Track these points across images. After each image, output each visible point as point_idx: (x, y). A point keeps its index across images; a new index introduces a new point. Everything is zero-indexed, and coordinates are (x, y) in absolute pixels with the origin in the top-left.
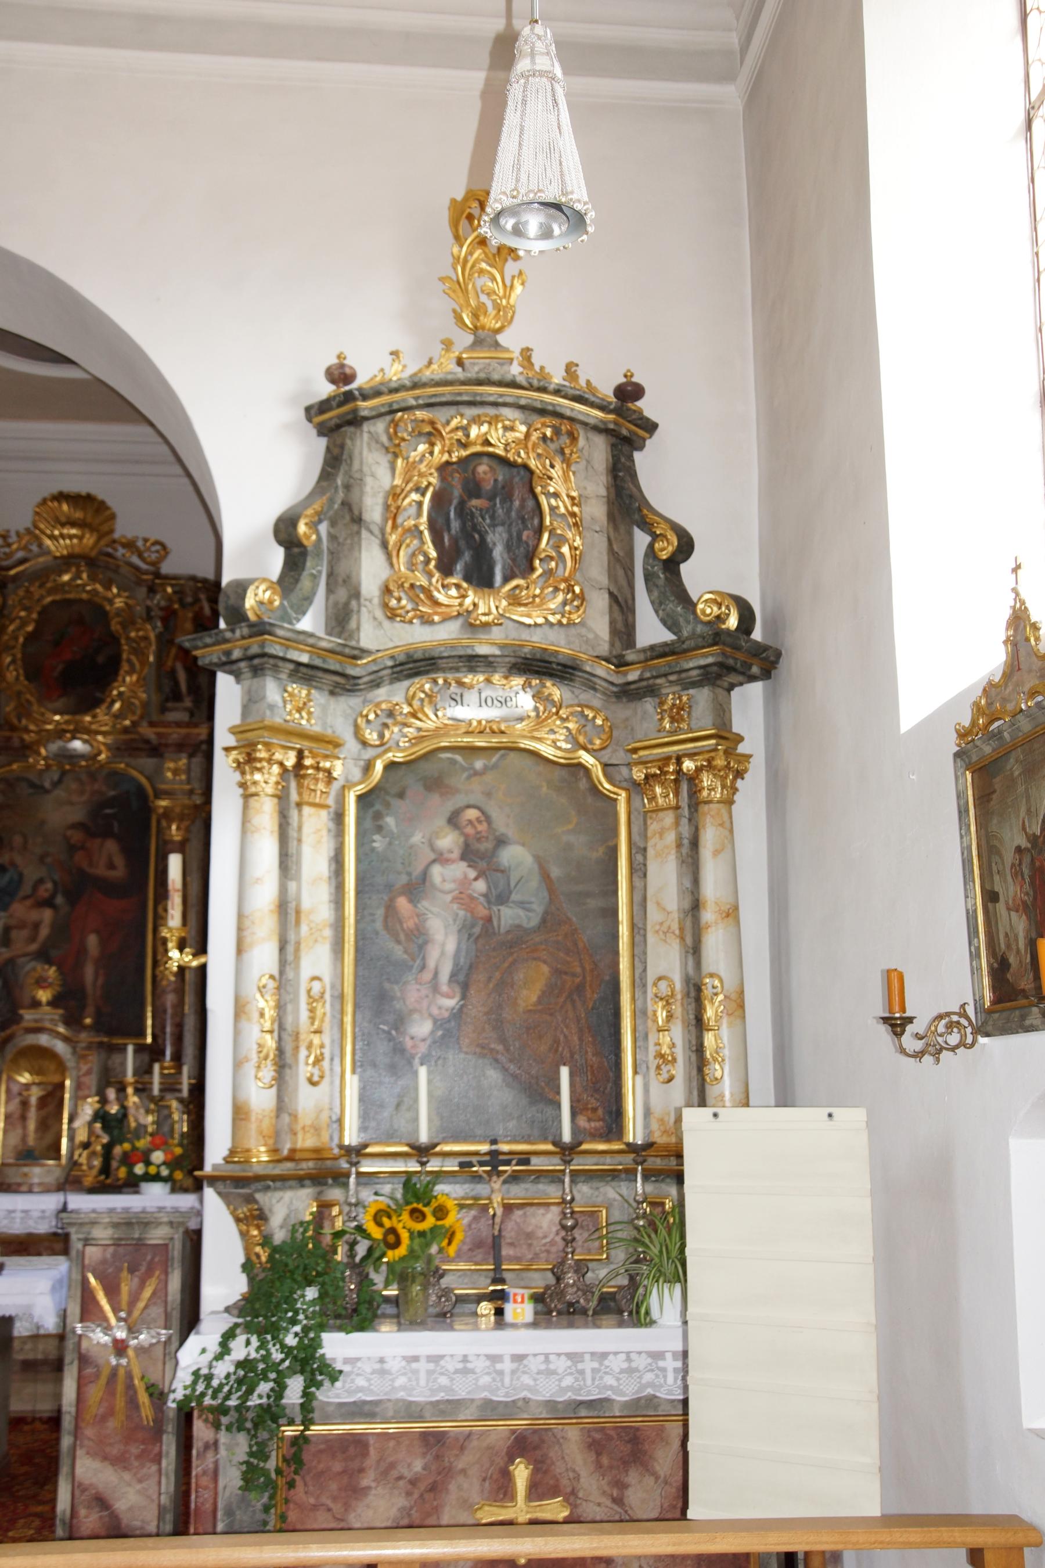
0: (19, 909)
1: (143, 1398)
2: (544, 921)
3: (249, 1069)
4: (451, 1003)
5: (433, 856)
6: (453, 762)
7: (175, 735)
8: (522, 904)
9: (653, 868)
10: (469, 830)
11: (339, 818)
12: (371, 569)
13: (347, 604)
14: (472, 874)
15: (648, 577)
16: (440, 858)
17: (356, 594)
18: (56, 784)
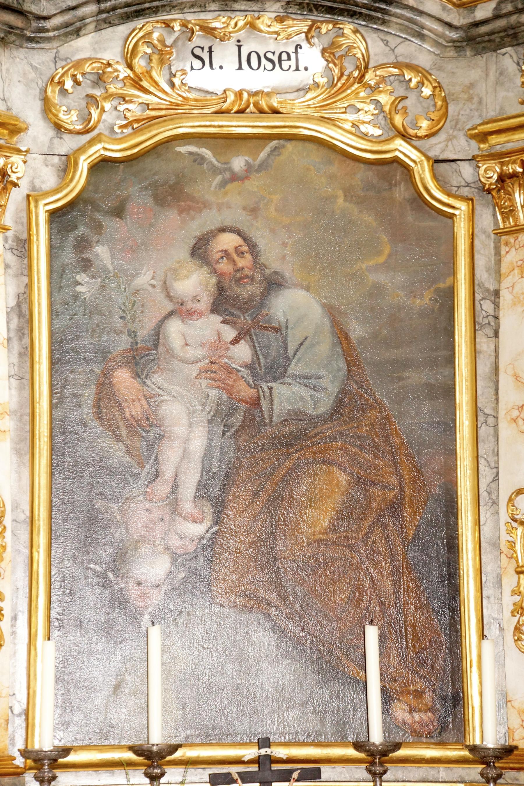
2: (339, 406)
4: (198, 529)
5: (169, 307)
6: (199, 159)
8: (305, 380)
10: (224, 266)
11: (23, 247)
14: (230, 333)
16: (180, 310)
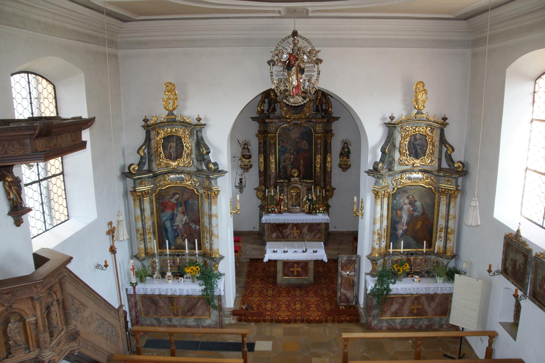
0: (287, 155)
1: (351, 282)
3: (375, 243)
4: (405, 228)
7: (319, 121)
8: (418, 212)
9: (441, 206)
12: (397, 155)
13: (392, 161)
15: (446, 156)
16: (405, 204)
17: (394, 160)
18: (293, 129)
